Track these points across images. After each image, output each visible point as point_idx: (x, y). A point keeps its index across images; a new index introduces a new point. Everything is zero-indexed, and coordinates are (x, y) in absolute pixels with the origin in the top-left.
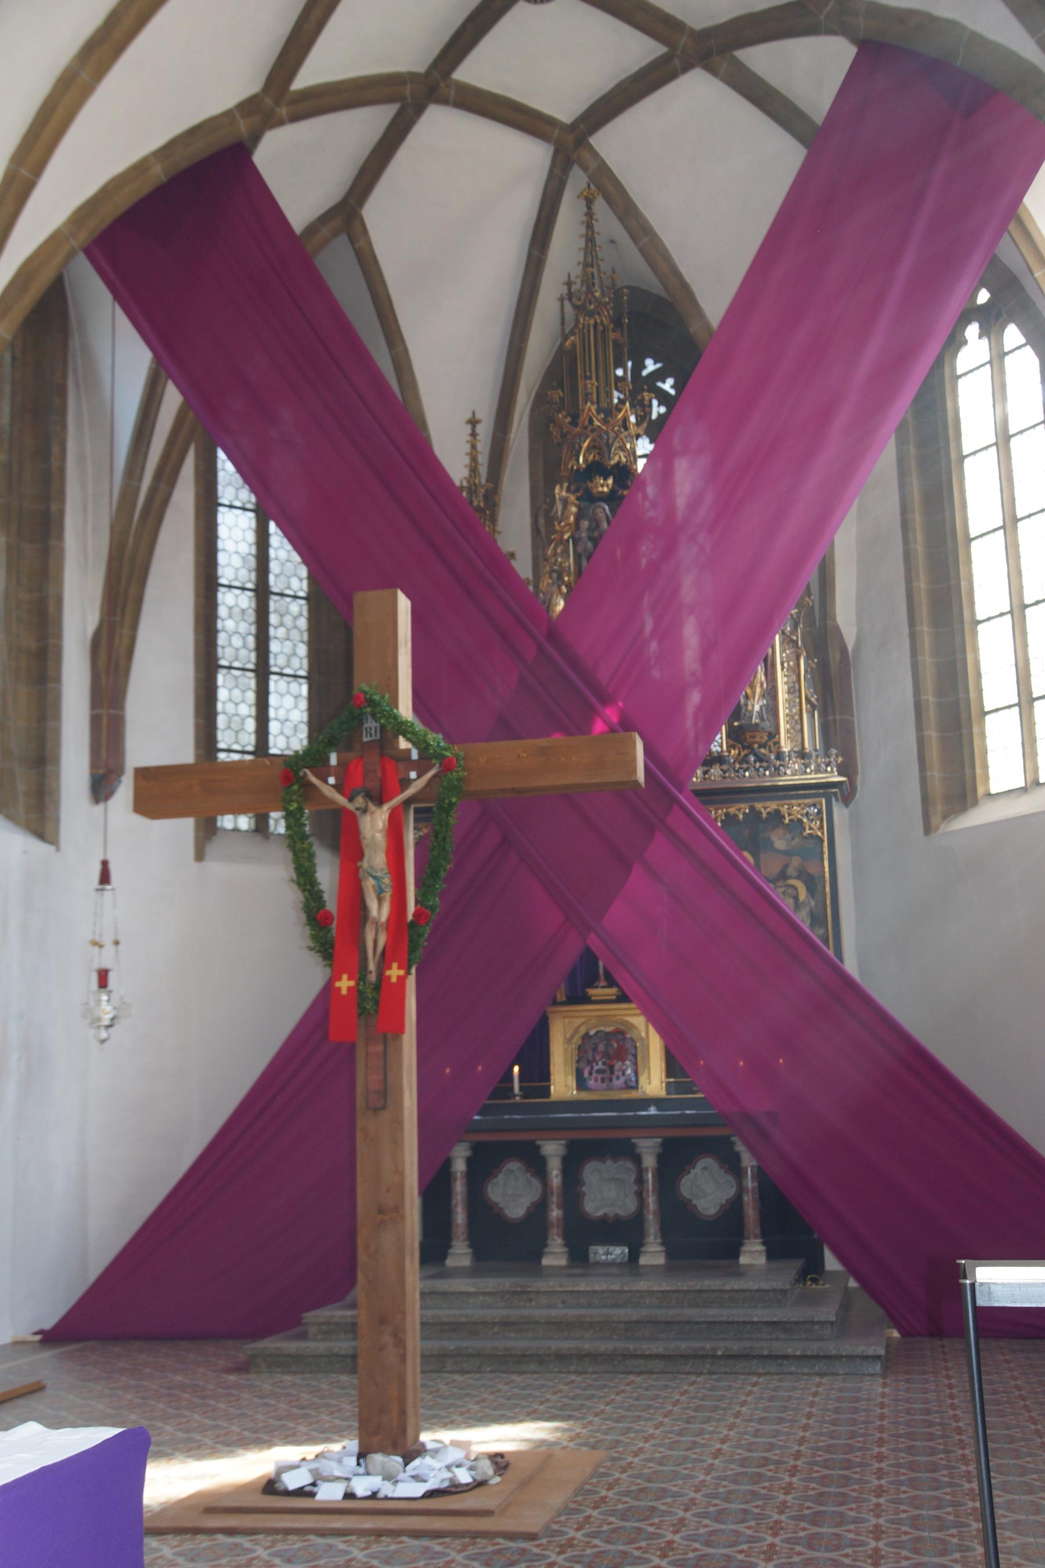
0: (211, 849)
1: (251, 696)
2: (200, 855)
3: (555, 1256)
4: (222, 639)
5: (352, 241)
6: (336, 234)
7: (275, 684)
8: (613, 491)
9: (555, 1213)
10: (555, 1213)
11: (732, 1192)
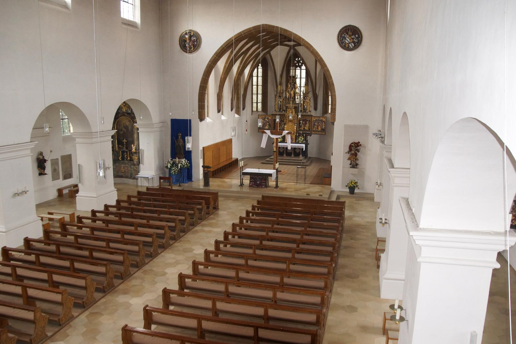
0: (253, 113)
1: (256, 97)
2: (252, 115)
3: (285, 155)
4: (253, 91)
5: (269, 54)
6: (267, 54)
7: (259, 95)
8: (294, 84)
9: (285, 152)
10: (285, 152)
11: (299, 151)
